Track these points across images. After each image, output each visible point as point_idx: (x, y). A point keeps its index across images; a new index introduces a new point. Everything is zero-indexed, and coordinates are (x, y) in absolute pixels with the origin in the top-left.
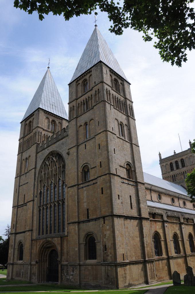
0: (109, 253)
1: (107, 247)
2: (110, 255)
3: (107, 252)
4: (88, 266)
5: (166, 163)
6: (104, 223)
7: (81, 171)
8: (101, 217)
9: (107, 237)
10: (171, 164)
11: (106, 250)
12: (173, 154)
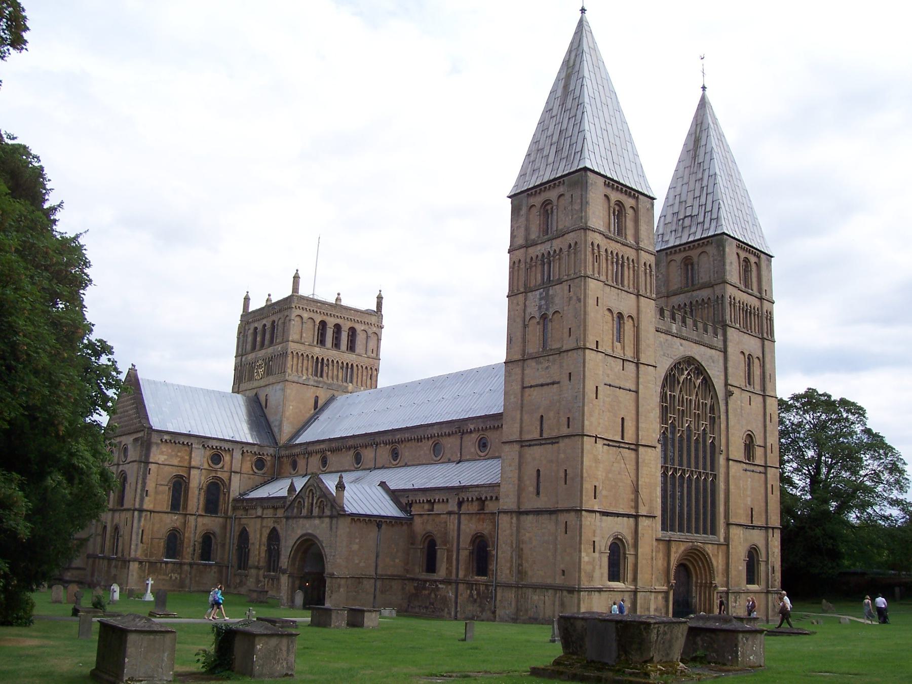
5: (312, 315)
10: (323, 324)
12: (332, 300)
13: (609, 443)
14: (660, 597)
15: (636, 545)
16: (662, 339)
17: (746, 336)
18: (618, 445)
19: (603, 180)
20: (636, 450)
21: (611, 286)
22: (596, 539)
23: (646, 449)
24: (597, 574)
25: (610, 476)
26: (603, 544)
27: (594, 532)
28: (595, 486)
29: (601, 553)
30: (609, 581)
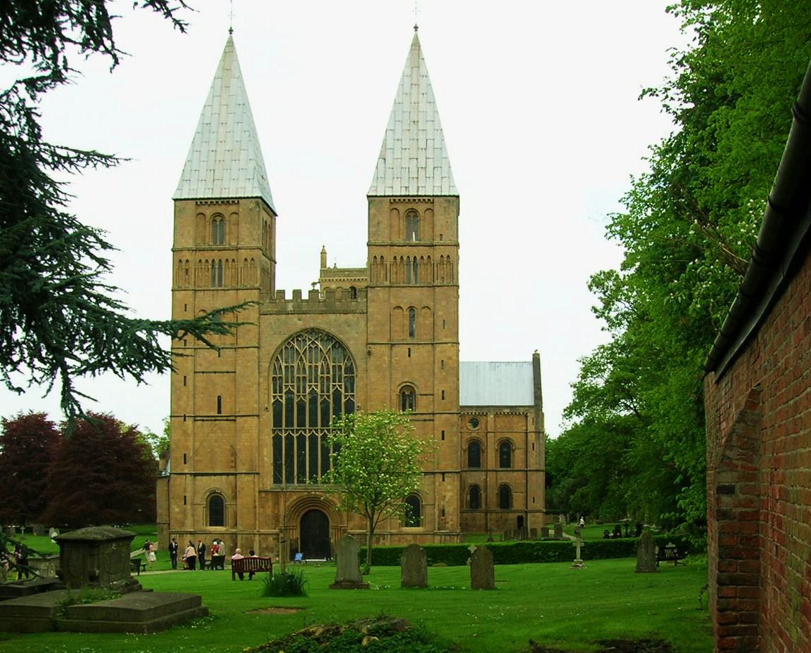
0: (448, 520)
1: (446, 511)
2: (451, 523)
3: (445, 519)
4: (406, 536)
6: (443, 480)
7: (398, 393)
8: (439, 473)
9: (447, 500)
11: (443, 516)
13: (205, 419)
14: (271, 539)
15: (235, 498)
16: (272, 321)
17: (404, 290)
18: (213, 419)
19: (194, 202)
20: (235, 420)
21: (204, 290)
22: (188, 495)
23: (246, 418)
24: (189, 522)
25: (205, 444)
26: (202, 499)
27: (185, 489)
28: (185, 455)
29: (193, 504)
30: (211, 525)
